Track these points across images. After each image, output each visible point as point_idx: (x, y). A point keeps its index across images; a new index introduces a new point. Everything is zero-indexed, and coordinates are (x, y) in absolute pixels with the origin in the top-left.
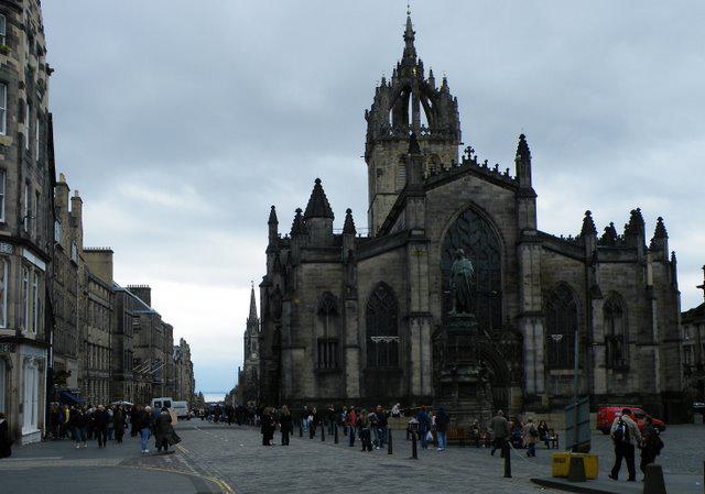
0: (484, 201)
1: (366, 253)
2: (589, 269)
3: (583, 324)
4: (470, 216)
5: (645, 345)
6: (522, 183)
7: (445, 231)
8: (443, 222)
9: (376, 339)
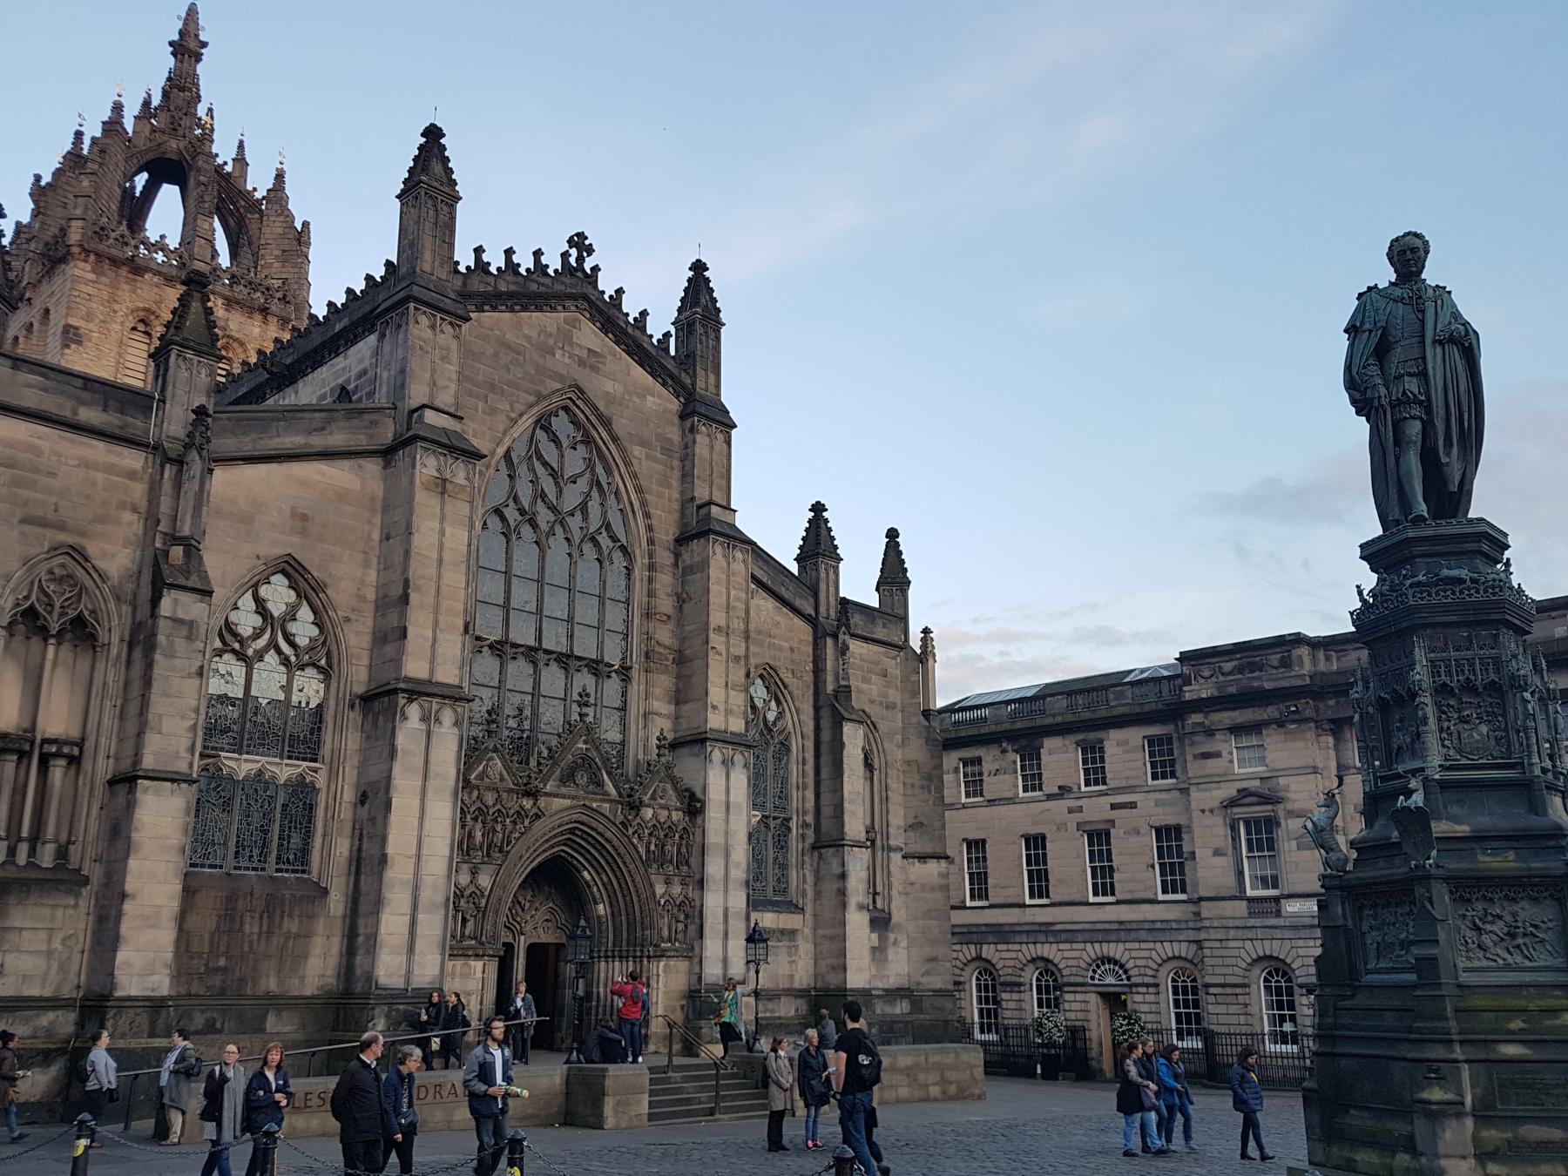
0: (610, 398)
1: (247, 444)
2: (829, 642)
3: (805, 788)
4: (561, 424)
5: (923, 858)
6: (700, 384)
7: (501, 451)
8: (501, 423)
9: (242, 766)
